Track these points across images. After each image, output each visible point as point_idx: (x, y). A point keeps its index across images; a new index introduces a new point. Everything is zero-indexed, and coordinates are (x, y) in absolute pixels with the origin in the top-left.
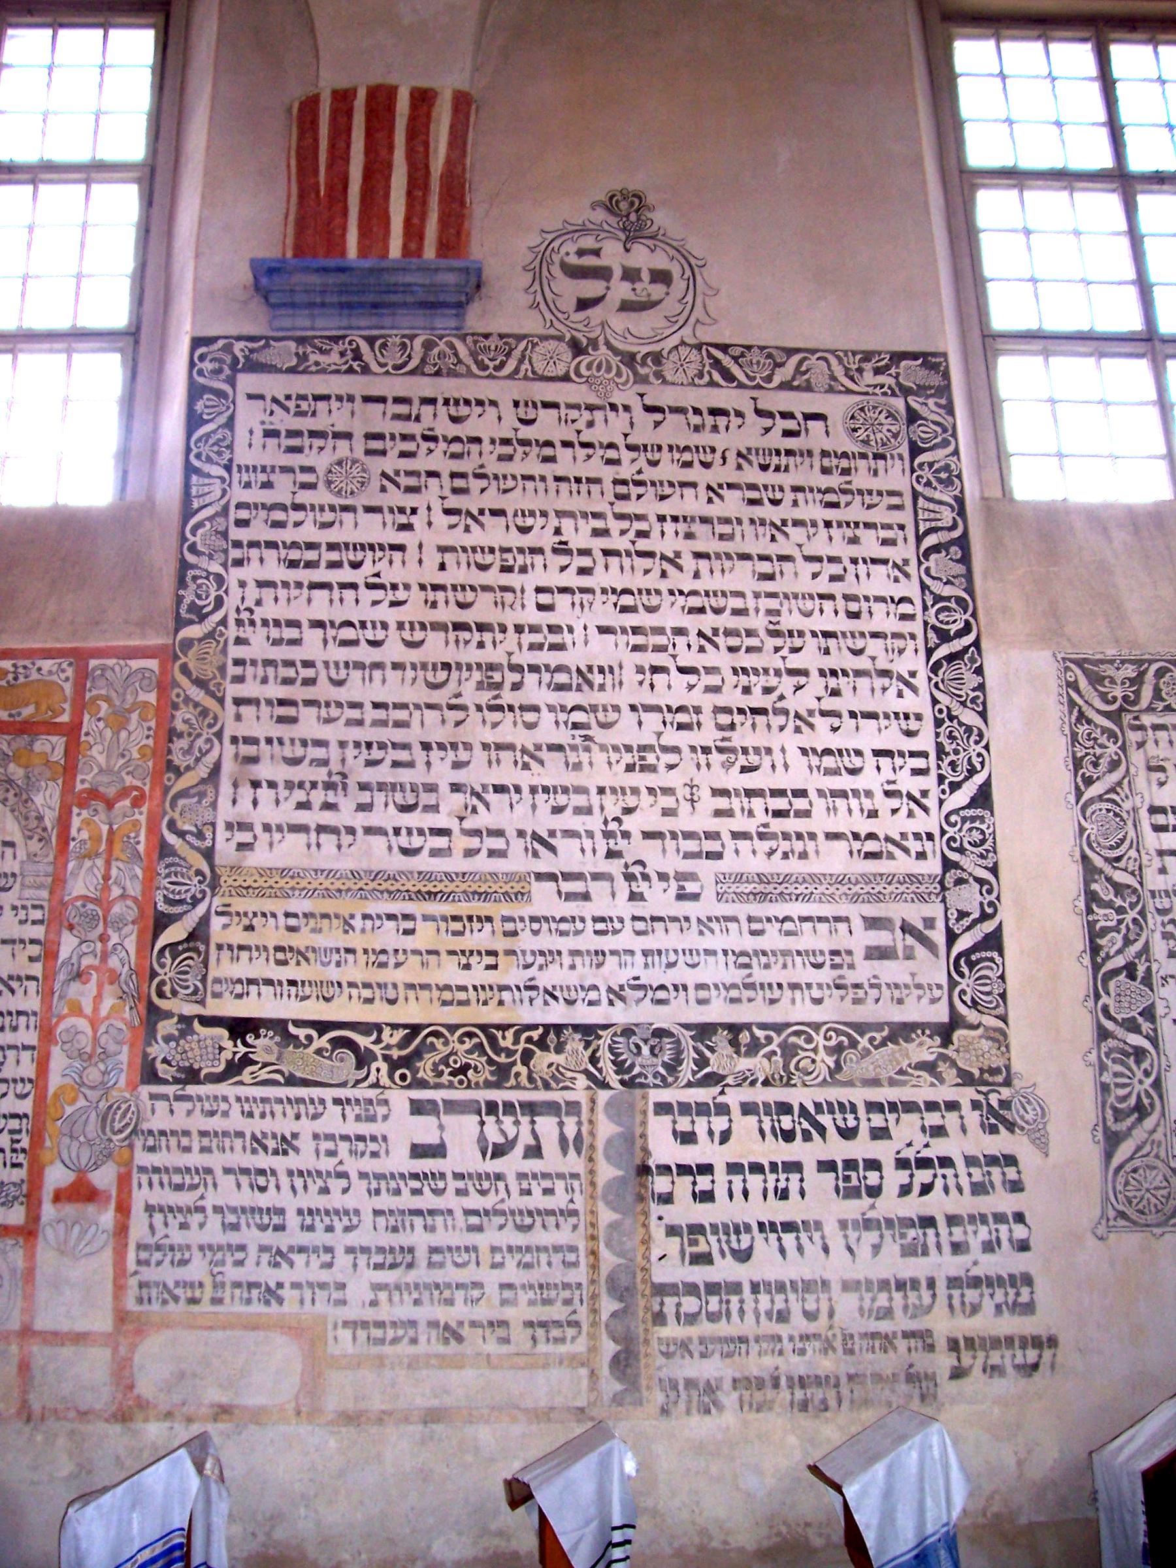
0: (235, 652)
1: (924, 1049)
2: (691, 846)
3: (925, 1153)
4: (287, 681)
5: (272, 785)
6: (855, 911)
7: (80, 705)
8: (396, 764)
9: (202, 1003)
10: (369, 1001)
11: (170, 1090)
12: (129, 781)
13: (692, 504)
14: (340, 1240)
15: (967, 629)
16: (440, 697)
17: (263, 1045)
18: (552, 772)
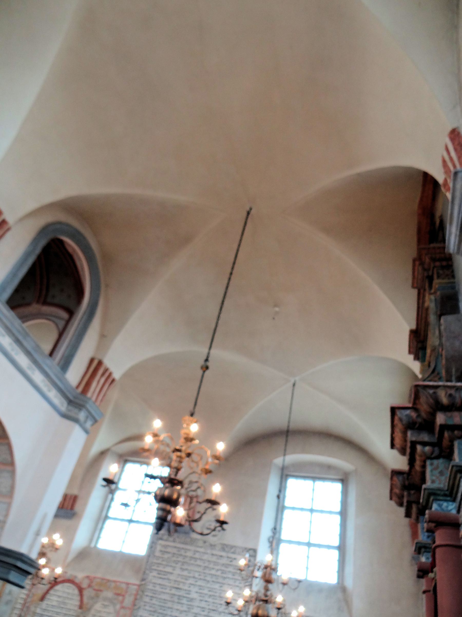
7: (126, 592)
13: (213, 572)
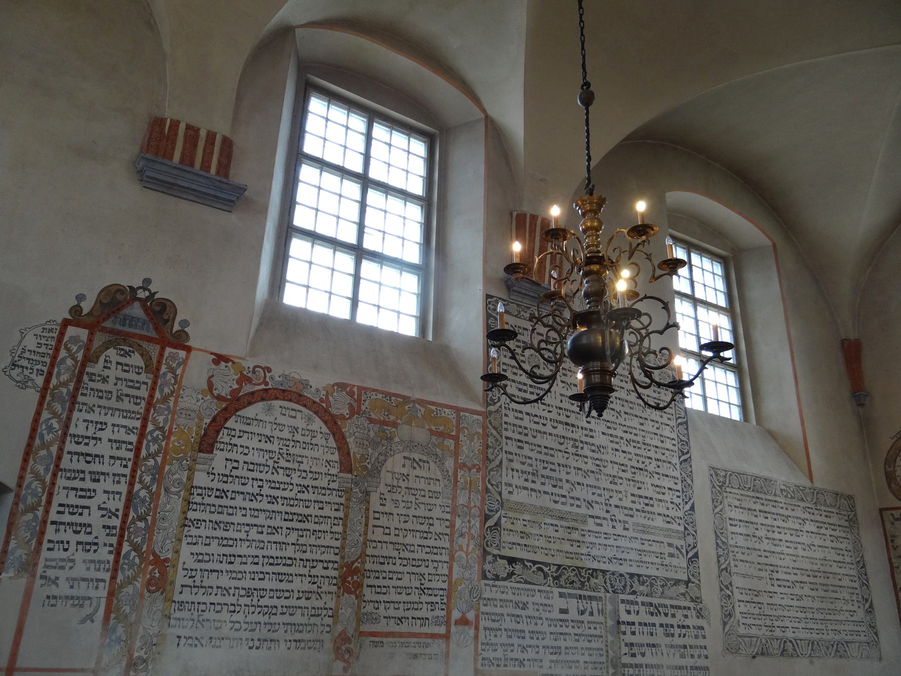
0: (505, 419)
1: (682, 589)
2: (626, 512)
3: (684, 624)
4: (520, 433)
5: (517, 471)
6: (666, 540)
7: (459, 430)
8: (551, 470)
9: (499, 550)
10: (547, 555)
11: (491, 582)
12: (476, 462)
14: (541, 643)
15: (687, 453)
16: (562, 448)
17: (518, 567)
18: (591, 481)
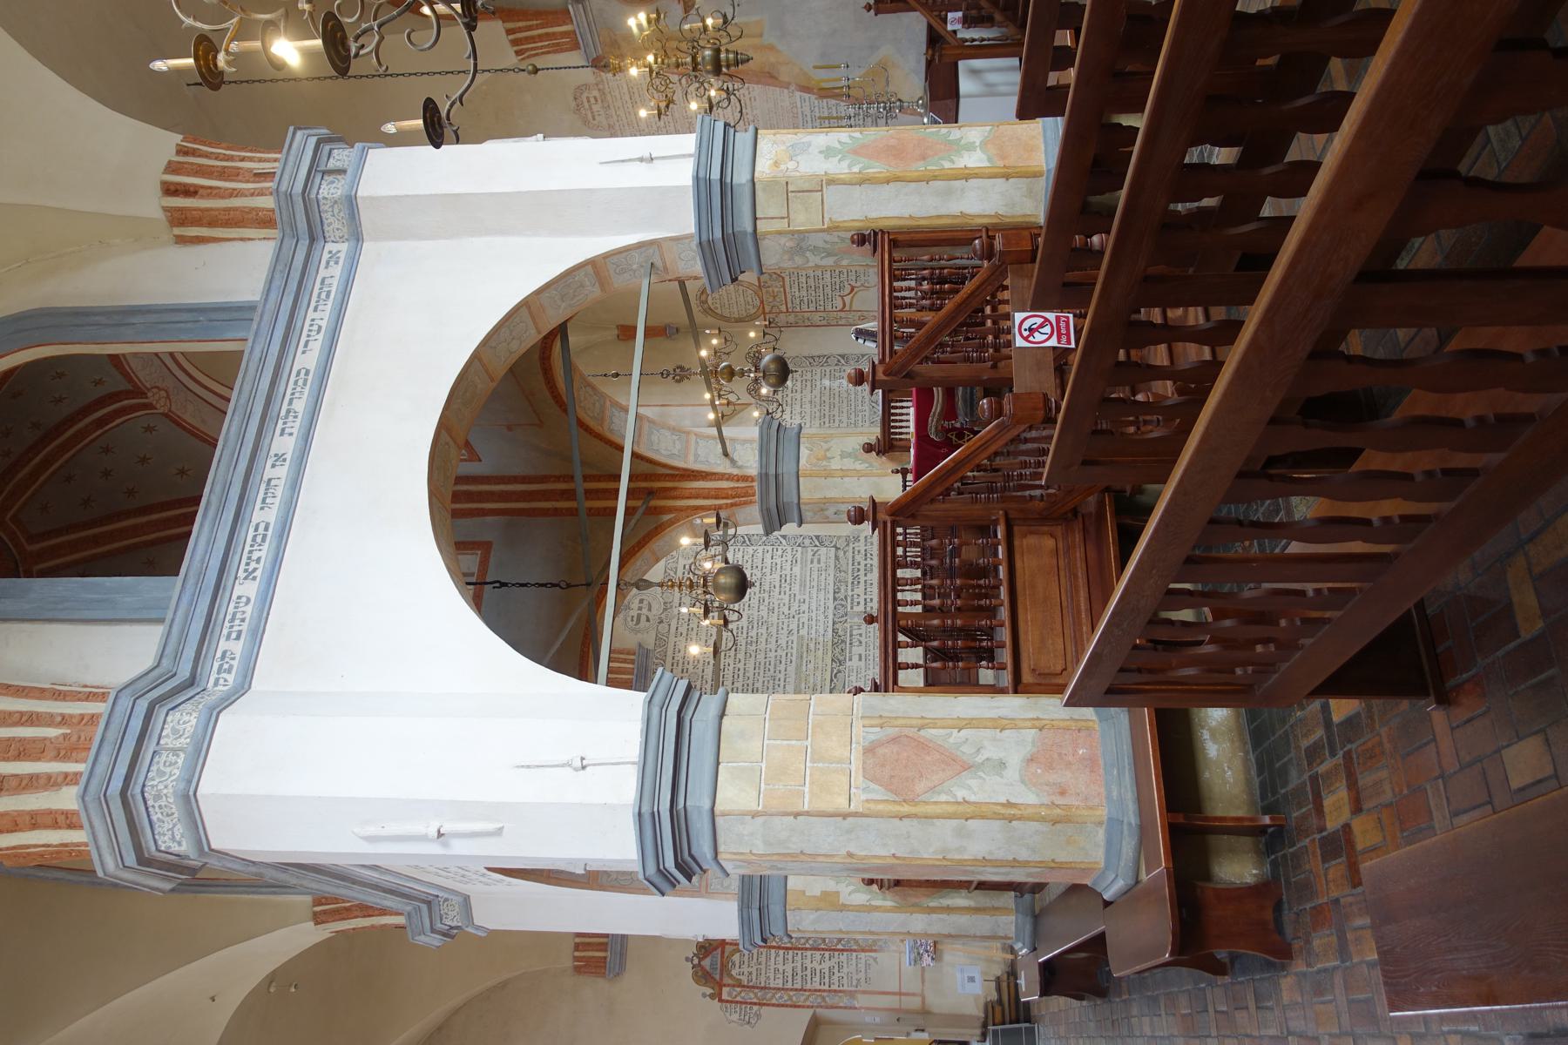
1: (841, 553)
18: (773, 630)
